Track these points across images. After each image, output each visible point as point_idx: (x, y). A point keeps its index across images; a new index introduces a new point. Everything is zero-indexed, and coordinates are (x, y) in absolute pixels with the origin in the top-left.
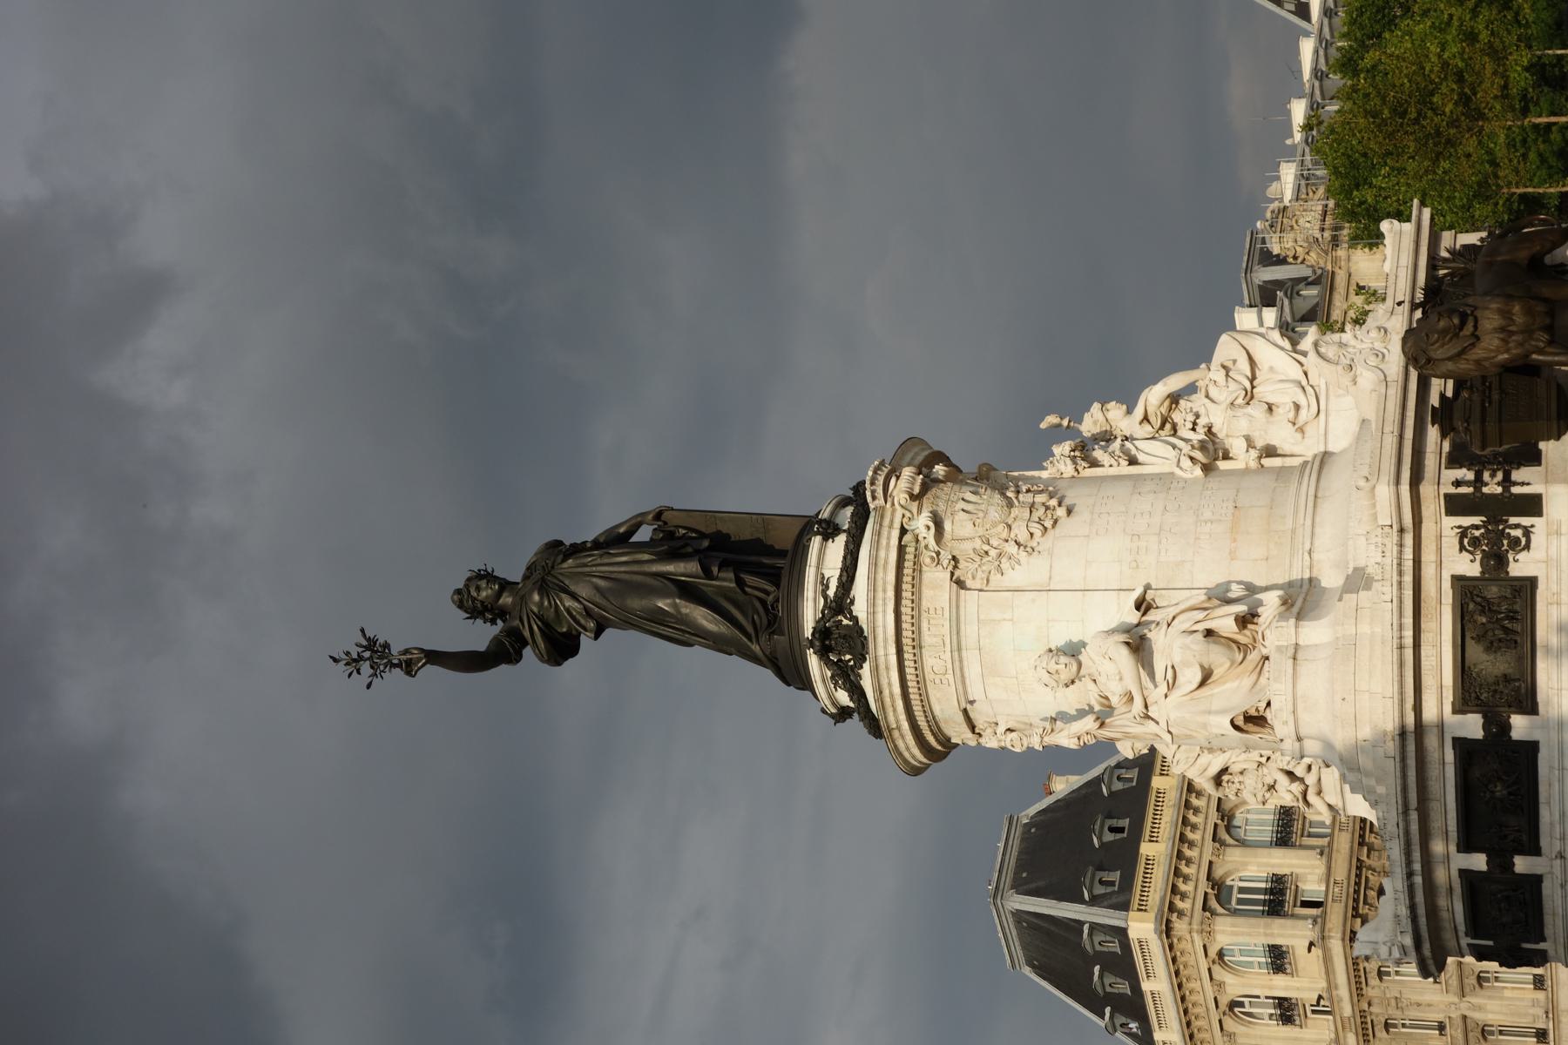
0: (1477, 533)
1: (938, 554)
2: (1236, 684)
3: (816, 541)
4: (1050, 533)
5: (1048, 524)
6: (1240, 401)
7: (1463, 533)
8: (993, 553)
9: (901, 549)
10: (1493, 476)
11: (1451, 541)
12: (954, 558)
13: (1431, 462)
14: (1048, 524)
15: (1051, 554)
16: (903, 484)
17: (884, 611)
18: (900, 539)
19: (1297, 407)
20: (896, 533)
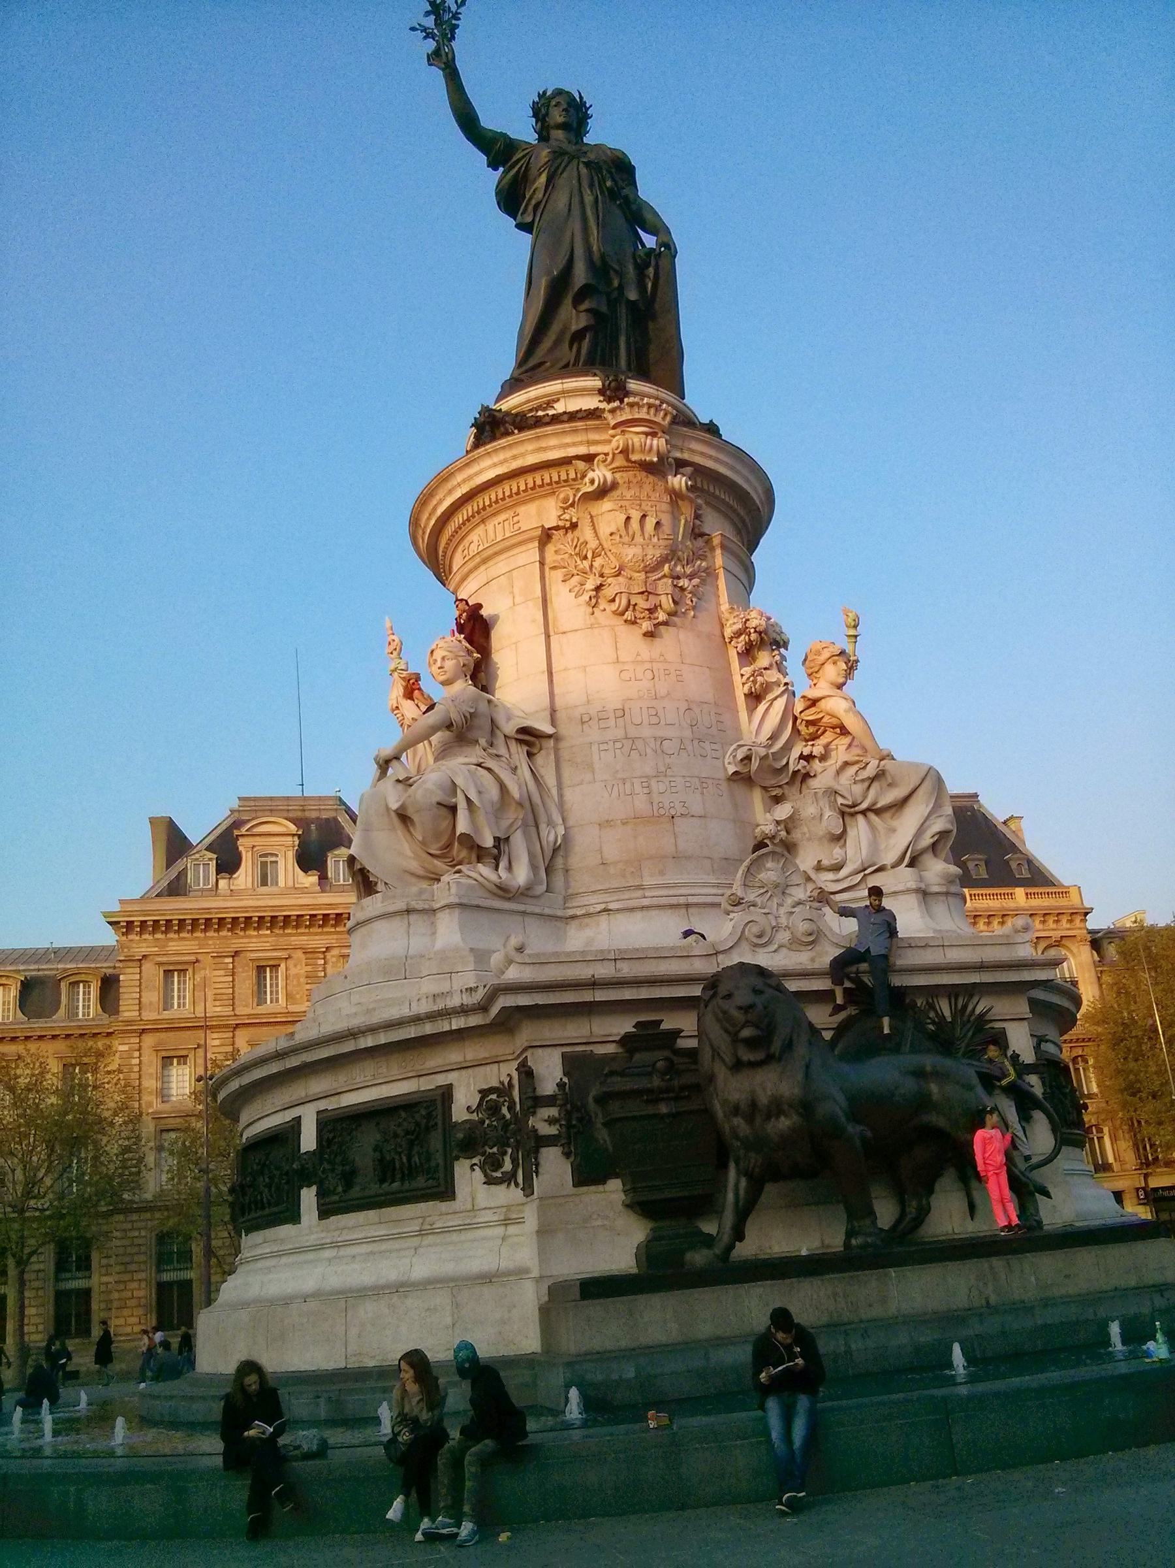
0: (505, 1110)
1: (572, 505)
2: (409, 853)
3: (596, 383)
4: (619, 621)
5: (629, 615)
6: (840, 800)
7: (503, 1091)
8: (586, 564)
9: (566, 461)
10: (551, 1121)
11: (492, 1076)
12: (574, 526)
13: (574, 1031)
14: (629, 615)
15: (592, 627)
16: (637, 440)
17: (495, 465)
18: (578, 457)
19: (837, 868)
20: (582, 450)
